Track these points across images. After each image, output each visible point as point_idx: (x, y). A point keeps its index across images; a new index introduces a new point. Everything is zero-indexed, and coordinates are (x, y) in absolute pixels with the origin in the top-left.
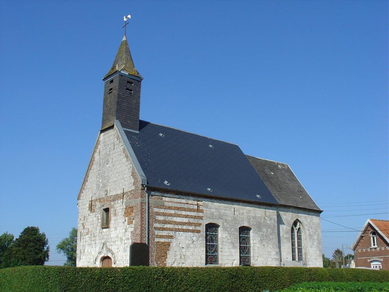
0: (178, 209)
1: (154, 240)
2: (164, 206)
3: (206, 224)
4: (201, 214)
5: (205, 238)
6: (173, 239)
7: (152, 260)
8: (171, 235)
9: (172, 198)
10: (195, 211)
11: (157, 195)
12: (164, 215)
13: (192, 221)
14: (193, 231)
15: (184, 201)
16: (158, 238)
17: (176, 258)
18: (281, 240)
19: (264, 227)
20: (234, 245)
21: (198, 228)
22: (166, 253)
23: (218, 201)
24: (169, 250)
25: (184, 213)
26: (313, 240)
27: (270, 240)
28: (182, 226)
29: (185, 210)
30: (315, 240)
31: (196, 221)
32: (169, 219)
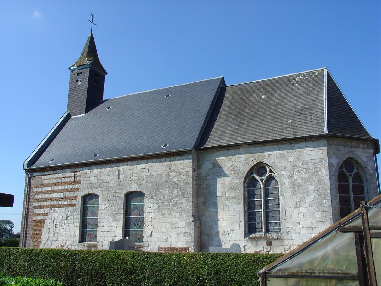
0: (55, 184)
1: (32, 219)
2: (42, 184)
3: (124, 193)
4: (78, 186)
5: (80, 212)
6: (48, 216)
7: (29, 238)
8: (47, 212)
9: (50, 175)
10: (71, 184)
11: (38, 175)
12: (42, 193)
13: (67, 194)
14: (68, 206)
15: (61, 175)
16: (35, 216)
17: (49, 235)
18: (218, 202)
19: (166, 188)
20: (116, 218)
21: (74, 202)
22: (41, 231)
23: (98, 166)
24: (43, 228)
25: (60, 188)
26: (304, 193)
27: (176, 205)
28: (57, 202)
29: (61, 184)
30: (308, 192)
31: (72, 194)
32: (46, 196)
